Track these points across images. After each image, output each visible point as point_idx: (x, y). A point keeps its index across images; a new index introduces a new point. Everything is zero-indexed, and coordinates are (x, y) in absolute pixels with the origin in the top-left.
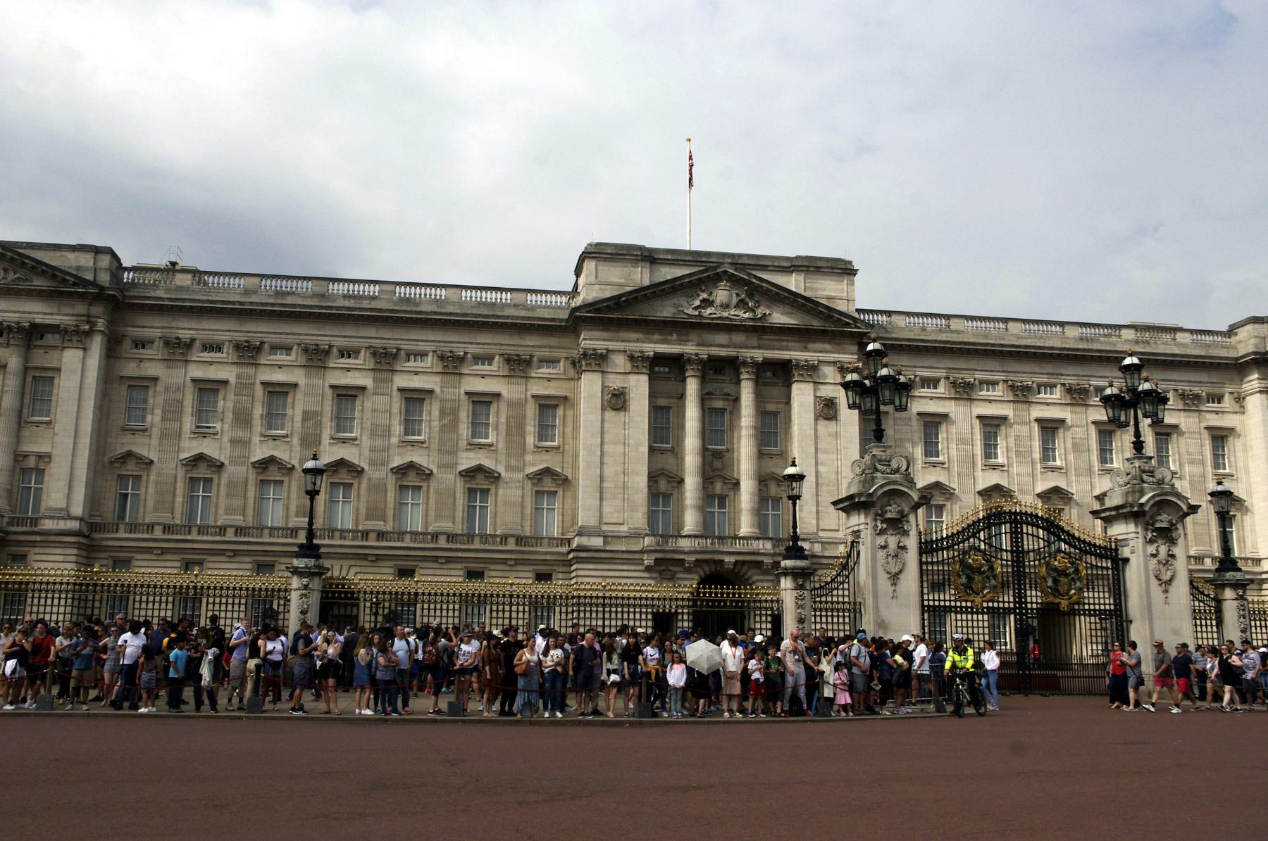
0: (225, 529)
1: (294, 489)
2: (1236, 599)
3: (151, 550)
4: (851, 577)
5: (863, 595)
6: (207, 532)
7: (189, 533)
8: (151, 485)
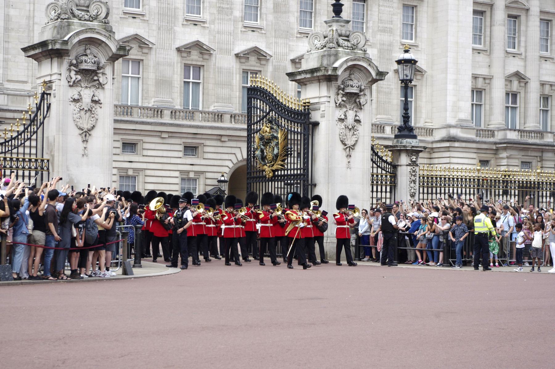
2: (409, 165)
4: (40, 131)
5: (51, 152)
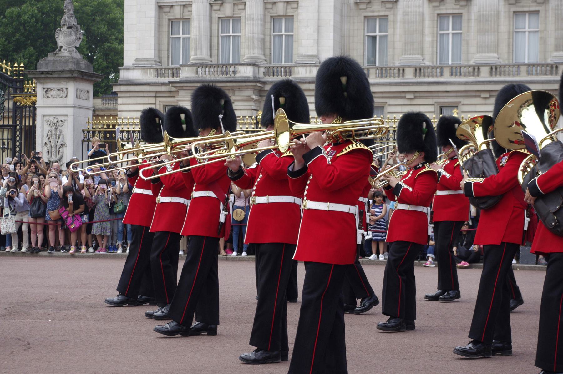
0: (479, 69)
1: (551, 18)
3: (403, 95)
6: (460, 72)
7: (442, 75)
8: (398, 25)
